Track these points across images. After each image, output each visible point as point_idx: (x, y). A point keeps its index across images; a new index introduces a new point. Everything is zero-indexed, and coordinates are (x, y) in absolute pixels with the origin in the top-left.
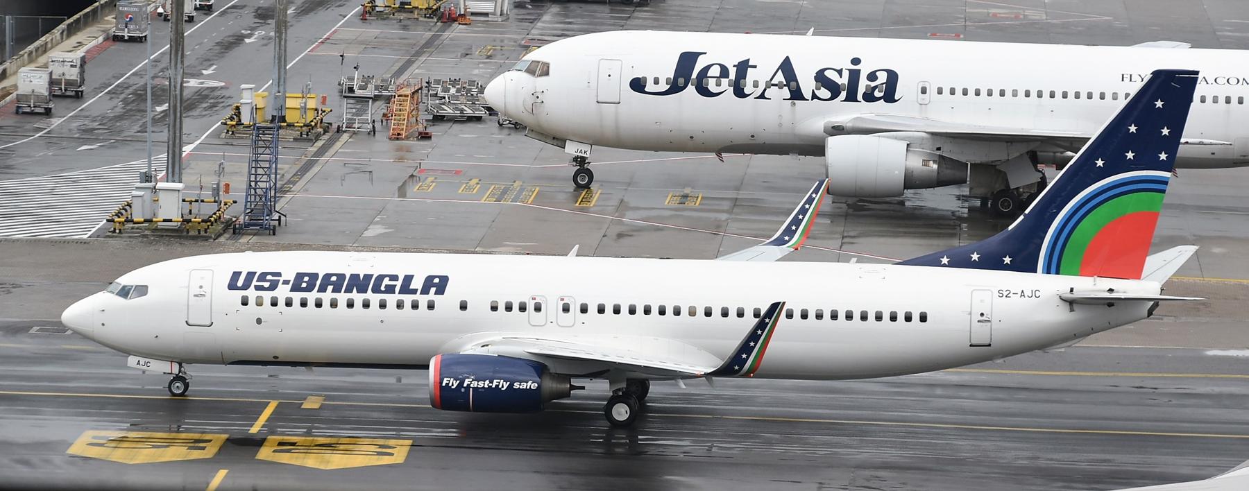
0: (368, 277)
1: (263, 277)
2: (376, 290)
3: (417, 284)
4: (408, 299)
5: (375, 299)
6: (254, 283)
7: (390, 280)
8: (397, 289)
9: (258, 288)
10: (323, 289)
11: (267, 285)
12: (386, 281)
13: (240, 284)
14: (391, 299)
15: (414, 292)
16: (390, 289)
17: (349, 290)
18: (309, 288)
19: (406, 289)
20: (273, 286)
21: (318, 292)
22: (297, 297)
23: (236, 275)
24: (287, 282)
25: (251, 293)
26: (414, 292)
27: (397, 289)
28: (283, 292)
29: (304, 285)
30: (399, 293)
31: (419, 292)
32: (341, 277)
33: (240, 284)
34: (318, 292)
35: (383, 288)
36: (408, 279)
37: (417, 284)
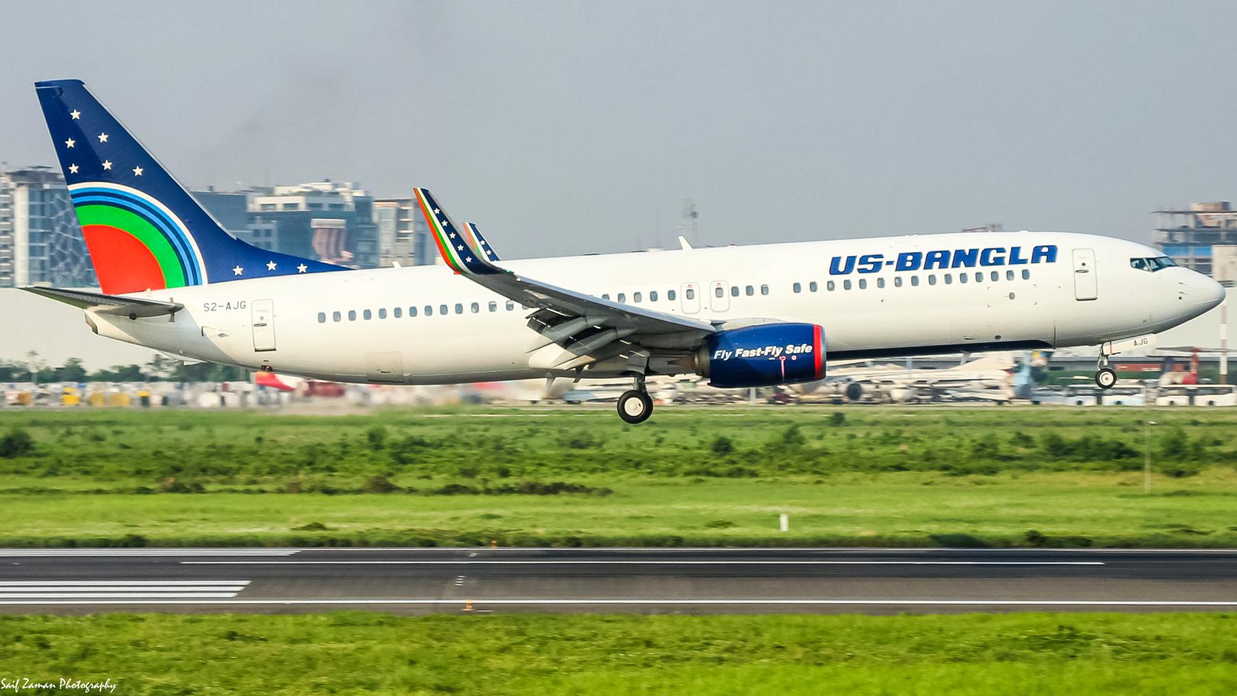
0: (973, 252)
1: (864, 260)
2: (985, 262)
3: (1026, 254)
4: (1017, 269)
5: (987, 271)
6: (857, 266)
7: (998, 252)
8: (1007, 260)
9: (860, 271)
10: (928, 266)
11: (870, 267)
12: (993, 254)
13: (842, 268)
14: (1002, 270)
15: (1024, 261)
16: (999, 261)
17: (955, 265)
18: (915, 265)
19: (1015, 259)
20: (877, 266)
21: (925, 268)
22: (906, 276)
23: (835, 261)
24: (889, 263)
25: (855, 277)
26: (1024, 261)
27: (1007, 260)
28: (888, 272)
29: (909, 264)
30: (1010, 263)
31: (1030, 261)
32: (946, 254)
33: (842, 268)
34: (925, 268)
35: (991, 261)
36: (1015, 251)
37: (1026, 254)
